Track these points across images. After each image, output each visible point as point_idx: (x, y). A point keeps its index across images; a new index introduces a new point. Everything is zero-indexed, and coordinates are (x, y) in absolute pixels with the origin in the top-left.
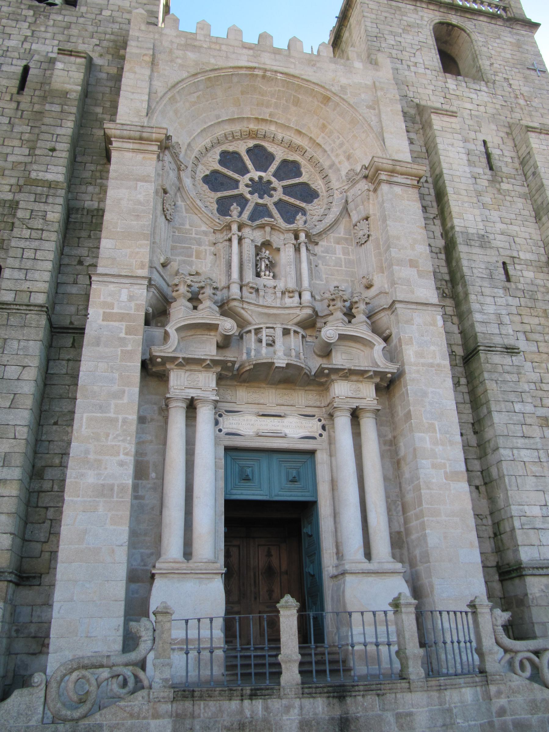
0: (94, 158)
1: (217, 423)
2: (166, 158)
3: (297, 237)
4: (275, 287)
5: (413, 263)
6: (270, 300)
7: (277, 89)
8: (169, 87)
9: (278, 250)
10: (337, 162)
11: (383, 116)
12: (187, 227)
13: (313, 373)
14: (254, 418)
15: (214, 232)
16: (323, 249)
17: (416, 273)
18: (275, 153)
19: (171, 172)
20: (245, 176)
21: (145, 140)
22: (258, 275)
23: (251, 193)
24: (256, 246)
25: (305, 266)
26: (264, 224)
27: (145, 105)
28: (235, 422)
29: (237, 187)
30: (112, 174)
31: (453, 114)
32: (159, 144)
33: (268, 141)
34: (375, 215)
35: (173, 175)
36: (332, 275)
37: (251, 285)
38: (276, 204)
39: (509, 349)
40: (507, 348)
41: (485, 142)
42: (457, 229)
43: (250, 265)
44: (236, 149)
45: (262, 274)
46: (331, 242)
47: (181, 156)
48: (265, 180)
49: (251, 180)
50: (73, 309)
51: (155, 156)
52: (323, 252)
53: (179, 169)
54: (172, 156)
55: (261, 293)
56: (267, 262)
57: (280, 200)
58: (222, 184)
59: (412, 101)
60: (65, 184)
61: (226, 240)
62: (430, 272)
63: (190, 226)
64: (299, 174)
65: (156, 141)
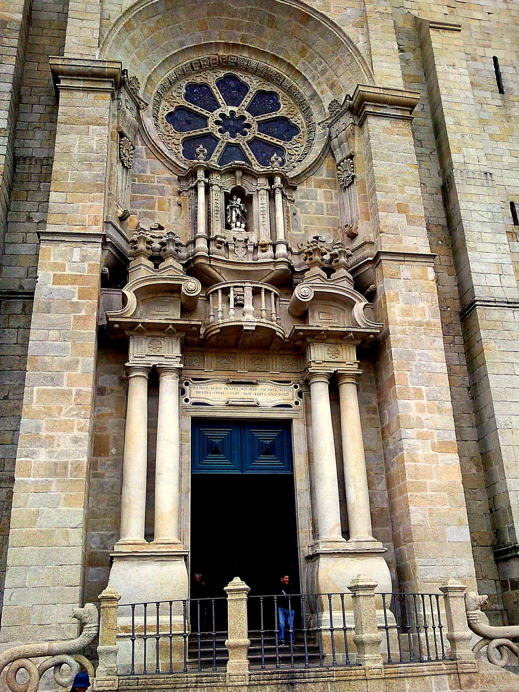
0: (42, 98)
1: (182, 392)
3: (271, 182)
4: (246, 241)
5: (401, 208)
6: (240, 256)
7: (249, 7)
8: (124, 11)
10: (319, 92)
11: (371, 35)
12: (149, 174)
13: (287, 336)
15: (179, 180)
16: (302, 194)
17: (405, 219)
19: (127, 111)
21: (97, 77)
22: (228, 227)
24: (225, 193)
25: (280, 214)
26: (234, 168)
27: (97, 34)
28: (203, 390)
30: (60, 118)
31: (456, 28)
32: (113, 80)
33: (240, 70)
34: (360, 153)
35: (130, 115)
36: (312, 224)
37: (218, 239)
38: (249, 143)
39: (511, 303)
40: (508, 303)
41: (495, 59)
42: (455, 166)
43: (218, 216)
44: (204, 81)
45: (233, 225)
47: (140, 93)
49: (222, 115)
50: (22, 272)
51: (109, 95)
52: (302, 198)
53: (138, 108)
54: (129, 93)
55: (231, 247)
56: (238, 212)
58: (188, 122)
59: (409, 12)
60: (8, 132)
61: (192, 188)
62: (421, 217)
63: (151, 172)
65: (108, 78)
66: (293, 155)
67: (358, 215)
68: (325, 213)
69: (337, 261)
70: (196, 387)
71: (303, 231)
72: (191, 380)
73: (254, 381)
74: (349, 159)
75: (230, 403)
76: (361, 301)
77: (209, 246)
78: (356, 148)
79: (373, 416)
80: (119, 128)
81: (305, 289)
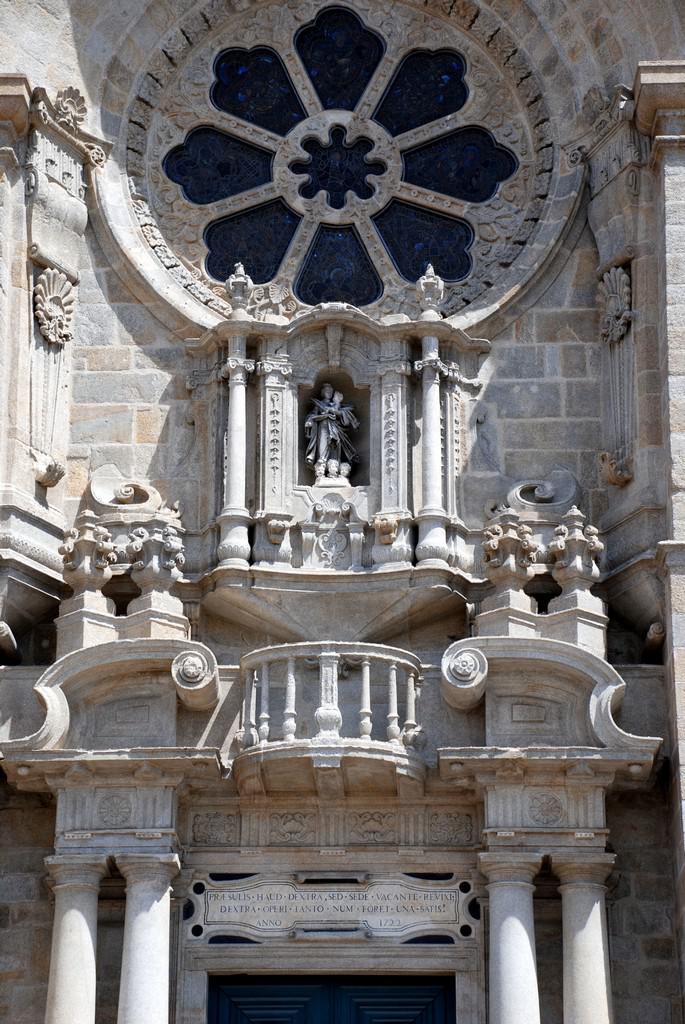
2: (37, 160)
9: (366, 393)
10: (564, 56)
14: (288, 890)
18: (383, 32)
20: (291, 135)
22: (308, 476)
23: (307, 191)
29: (268, 178)
36: (525, 445)
37: (273, 522)
38: (378, 218)
44: (264, 41)
45: (320, 469)
46: (529, 336)
48: (349, 138)
49: (310, 143)
56: (334, 431)
57: (395, 203)
64: (456, 97)
66: (494, 241)
67: (634, 426)
68: (563, 412)
69: (562, 568)
70: (221, 894)
71: (503, 468)
72: (210, 880)
73: (360, 878)
74: (620, 270)
75: (300, 935)
76: (608, 682)
77: (251, 541)
78: (641, 236)
79: (664, 963)
80: (32, 248)
81: (467, 657)
